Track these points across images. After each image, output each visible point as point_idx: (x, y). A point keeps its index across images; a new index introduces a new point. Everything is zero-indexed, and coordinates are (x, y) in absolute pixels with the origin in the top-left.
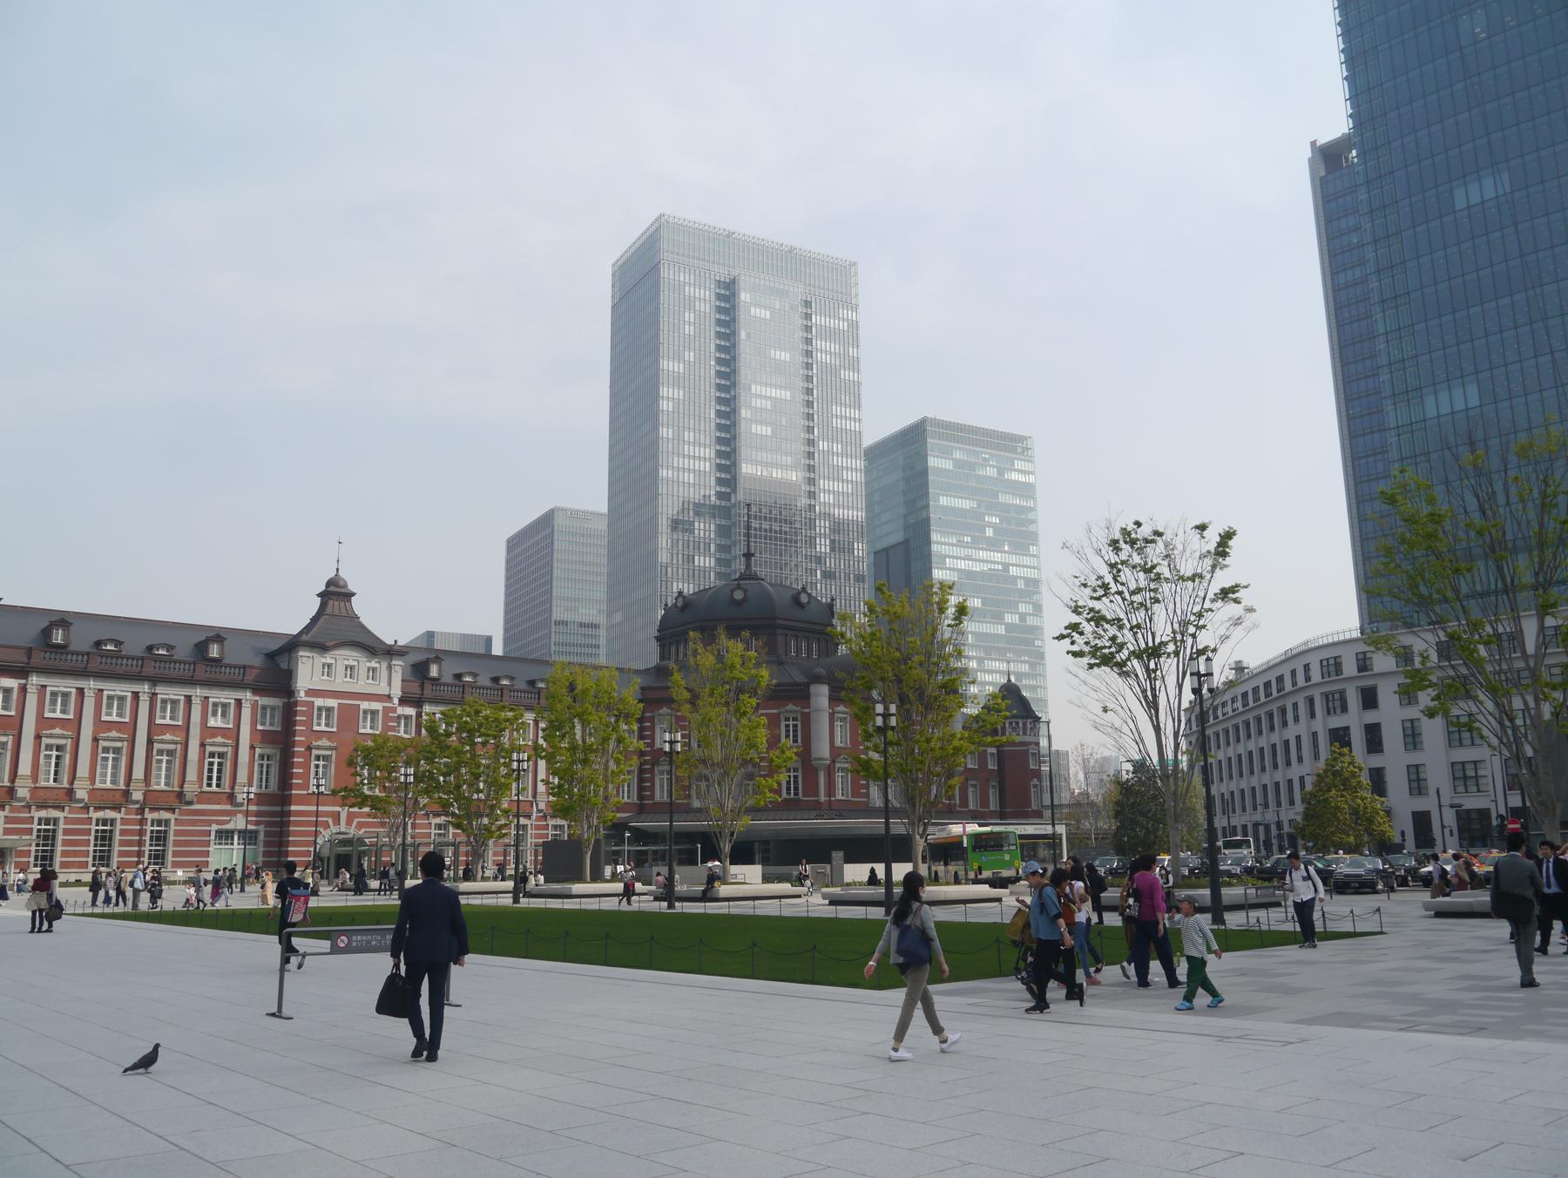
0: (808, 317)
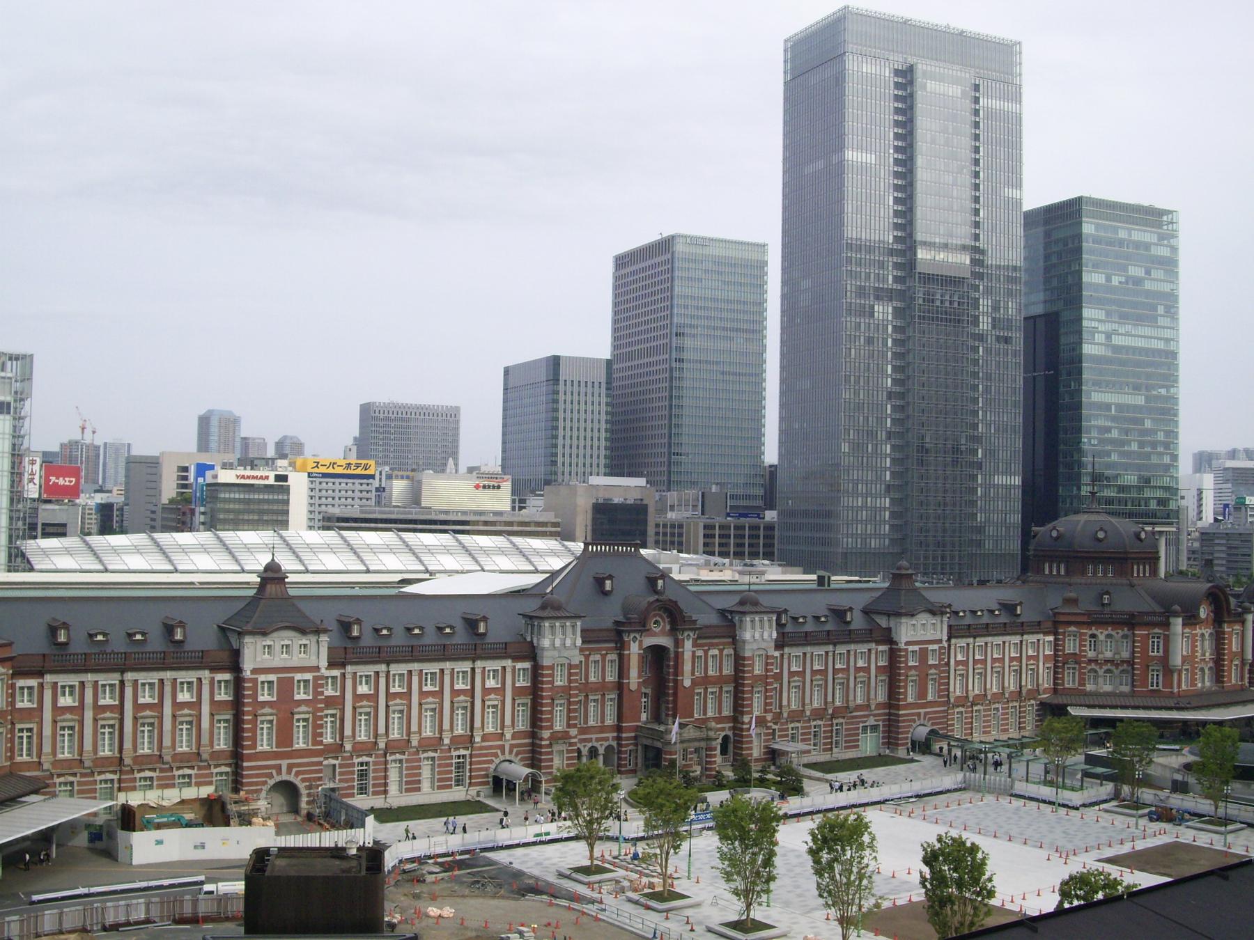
0: (976, 100)
